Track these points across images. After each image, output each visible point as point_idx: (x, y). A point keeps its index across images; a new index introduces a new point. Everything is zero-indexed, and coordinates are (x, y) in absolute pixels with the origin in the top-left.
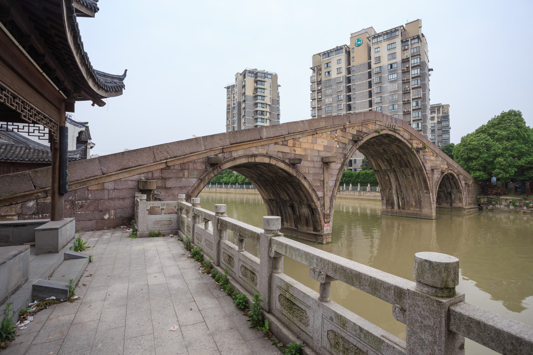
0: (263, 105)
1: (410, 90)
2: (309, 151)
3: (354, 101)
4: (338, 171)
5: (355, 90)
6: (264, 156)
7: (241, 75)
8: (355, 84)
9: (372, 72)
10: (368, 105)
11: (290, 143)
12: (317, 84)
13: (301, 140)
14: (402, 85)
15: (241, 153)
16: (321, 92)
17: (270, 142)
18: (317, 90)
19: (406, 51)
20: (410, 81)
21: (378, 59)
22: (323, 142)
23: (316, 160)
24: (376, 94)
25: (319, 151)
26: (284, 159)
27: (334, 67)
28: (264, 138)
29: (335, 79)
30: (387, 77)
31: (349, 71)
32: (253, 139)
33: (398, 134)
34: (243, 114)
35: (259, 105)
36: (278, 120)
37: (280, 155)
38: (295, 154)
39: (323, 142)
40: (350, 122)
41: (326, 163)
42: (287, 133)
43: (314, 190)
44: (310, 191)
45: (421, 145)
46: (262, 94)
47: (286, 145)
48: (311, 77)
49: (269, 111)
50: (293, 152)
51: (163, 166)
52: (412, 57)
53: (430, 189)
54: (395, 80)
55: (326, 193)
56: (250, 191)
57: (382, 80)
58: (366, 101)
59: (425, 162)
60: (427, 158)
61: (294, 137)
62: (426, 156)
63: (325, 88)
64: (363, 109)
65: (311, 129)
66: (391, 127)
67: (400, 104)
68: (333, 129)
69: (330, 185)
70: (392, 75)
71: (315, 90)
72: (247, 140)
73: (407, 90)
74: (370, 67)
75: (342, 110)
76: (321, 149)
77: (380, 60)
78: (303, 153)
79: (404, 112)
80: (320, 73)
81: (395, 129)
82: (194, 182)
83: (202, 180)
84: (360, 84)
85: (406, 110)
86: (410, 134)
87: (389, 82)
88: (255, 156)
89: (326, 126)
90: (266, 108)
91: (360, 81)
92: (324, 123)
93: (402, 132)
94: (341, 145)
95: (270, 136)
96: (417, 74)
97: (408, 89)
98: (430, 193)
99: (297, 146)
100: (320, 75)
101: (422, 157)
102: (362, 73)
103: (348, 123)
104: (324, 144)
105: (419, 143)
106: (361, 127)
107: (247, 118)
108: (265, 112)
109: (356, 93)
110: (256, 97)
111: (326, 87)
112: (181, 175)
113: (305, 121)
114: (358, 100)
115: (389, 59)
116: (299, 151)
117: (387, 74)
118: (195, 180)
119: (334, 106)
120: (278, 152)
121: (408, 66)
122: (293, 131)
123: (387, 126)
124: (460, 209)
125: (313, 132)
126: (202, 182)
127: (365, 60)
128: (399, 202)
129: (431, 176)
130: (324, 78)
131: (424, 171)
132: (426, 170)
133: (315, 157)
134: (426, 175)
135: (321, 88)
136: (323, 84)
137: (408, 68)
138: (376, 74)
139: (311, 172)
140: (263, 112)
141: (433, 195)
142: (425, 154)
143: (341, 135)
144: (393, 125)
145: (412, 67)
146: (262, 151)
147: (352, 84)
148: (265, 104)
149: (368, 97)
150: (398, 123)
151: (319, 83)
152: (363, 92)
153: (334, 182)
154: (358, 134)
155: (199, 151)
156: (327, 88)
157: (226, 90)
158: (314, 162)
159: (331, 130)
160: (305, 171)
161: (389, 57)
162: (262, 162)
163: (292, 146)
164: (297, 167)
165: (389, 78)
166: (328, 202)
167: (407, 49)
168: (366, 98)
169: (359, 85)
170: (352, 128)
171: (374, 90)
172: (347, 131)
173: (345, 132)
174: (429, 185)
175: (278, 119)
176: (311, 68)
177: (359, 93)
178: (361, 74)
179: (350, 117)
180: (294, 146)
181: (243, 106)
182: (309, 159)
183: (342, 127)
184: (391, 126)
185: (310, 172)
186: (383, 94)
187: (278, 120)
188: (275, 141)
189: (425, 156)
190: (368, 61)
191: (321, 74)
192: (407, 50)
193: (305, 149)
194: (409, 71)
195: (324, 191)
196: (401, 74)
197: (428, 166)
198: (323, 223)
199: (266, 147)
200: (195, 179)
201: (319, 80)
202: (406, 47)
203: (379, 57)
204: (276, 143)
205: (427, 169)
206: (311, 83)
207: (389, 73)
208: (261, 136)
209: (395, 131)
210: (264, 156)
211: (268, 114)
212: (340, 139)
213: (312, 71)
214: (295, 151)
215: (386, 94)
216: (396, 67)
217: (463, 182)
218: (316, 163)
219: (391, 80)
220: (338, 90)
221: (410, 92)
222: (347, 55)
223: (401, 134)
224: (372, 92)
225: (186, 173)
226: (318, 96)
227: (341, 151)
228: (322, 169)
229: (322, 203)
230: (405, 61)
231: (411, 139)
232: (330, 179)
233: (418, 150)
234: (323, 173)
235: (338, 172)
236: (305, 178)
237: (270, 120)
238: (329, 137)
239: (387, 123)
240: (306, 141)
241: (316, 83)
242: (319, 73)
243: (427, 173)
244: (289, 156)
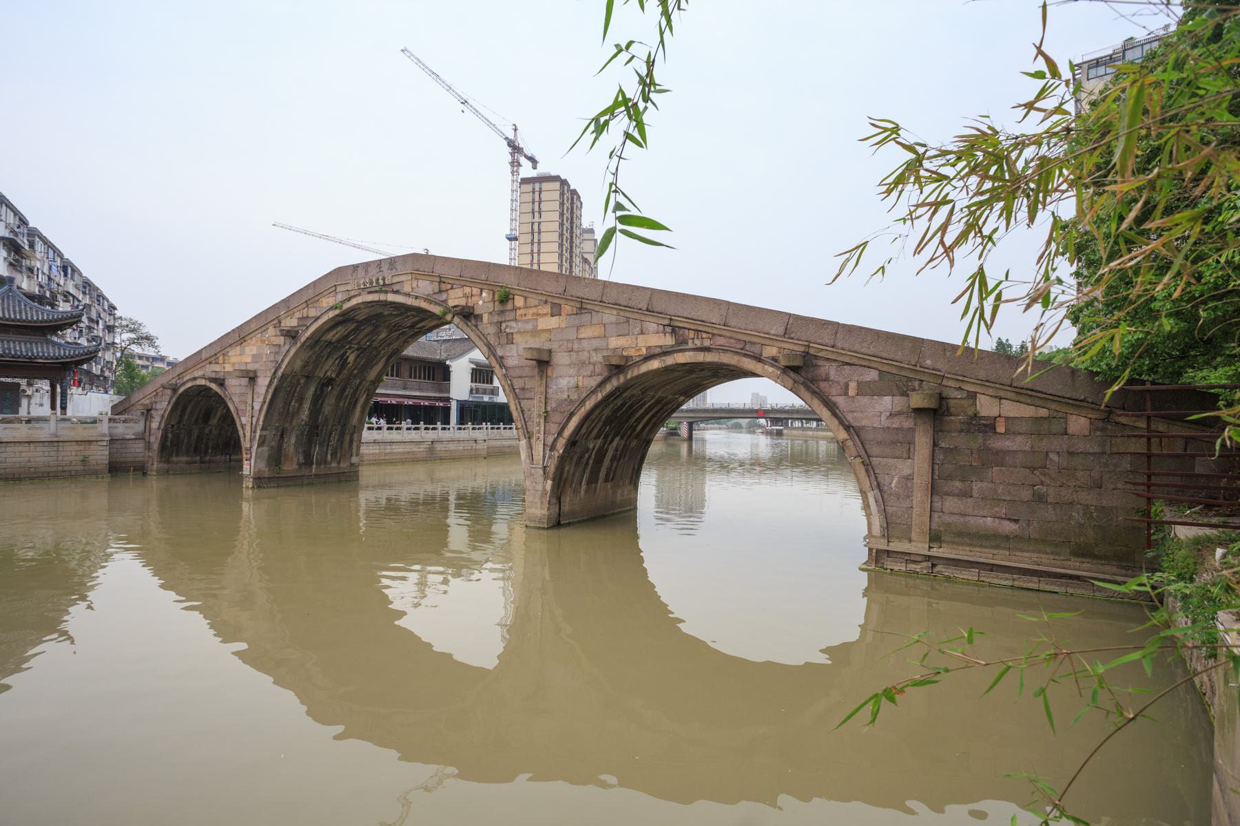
13: (229, 354)
25: (246, 363)
33: (397, 292)
39: (251, 350)
41: (252, 378)
45: (484, 294)
47: (218, 363)
51: (155, 393)
59: (504, 341)
60: (513, 327)
62: (513, 324)
66: (374, 284)
76: (249, 360)
81: (384, 285)
88: (195, 379)
93: (409, 283)
94: (273, 349)
104: (253, 353)
105: (476, 291)
106: (305, 311)
123: (362, 286)
142: (510, 316)
143: (274, 334)
144: (378, 279)
154: (301, 323)
184: (371, 283)
189: (504, 325)
199: (204, 369)
204: (210, 363)
205: (510, 362)
209: (385, 288)
214: (224, 368)
223: (407, 289)
227: (272, 358)
231: (440, 291)
236: (231, 399)
239: (362, 282)
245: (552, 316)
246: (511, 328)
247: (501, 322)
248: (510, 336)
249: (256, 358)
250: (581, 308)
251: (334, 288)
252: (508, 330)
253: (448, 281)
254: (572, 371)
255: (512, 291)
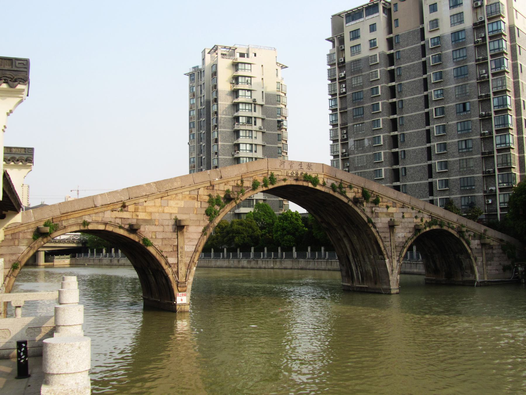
0: (250, 106)
1: (488, 77)
2: (157, 214)
3: (400, 96)
4: (201, 234)
5: (402, 78)
6: (98, 223)
7: (209, 53)
8: (401, 66)
9: (426, 46)
10: (423, 104)
11: (131, 208)
12: (339, 68)
14: (475, 69)
15: (71, 222)
16: (345, 81)
17: (105, 209)
18: (340, 79)
19: (479, 10)
20: (487, 62)
21: (435, 24)
22: (177, 204)
23: (167, 224)
24: (433, 85)
26: (123, 225)
27: (366, 36)
28: (98, 206)
29: (367, 59)
30: (451, 55)
31: (390, 43)
32: (85, 208)
34: (213, 123)
35: (241, 106)
36: (279, 132)
37: (119, 221)
38: (137, 219)
40: (221, 178)
42: (128, 198)
43: (163, 256)
44: (158, 257)
46: (247, 87)
48: (328, 55)
49: (260, 115)
50: (135, 217)
52: (489, 19)
53: (385, 253)
54: (463, 60)
55: (180, 259)
56: (220, 263)
57: (443, 60)
58: (421, 97)
59: (374, 215)
61: (136, 202)
62: (378, 208)
63: (351, 75)
64: (415, 112)
65: (159, 191)
67: (473, 102)
68: (194, 188)
69: (188, 250)
70: (458, 52)
71: (336, 79)
72: (79, 209)
73: (484, 77)
74: (423, 38)
75: (380, 114)
77: (437, 26)
78: (147, 217)
79: (481, 116)
80: (343, 48)
82: (24, 250)
83: (31, 248)
84: (409, 68)
85: (484, 113)
86: (340, 181)
87: (454, 64)
89: (183, 185)
90: (255, 111)
91: (409, 62)
92: (179, 183)
95: (106, 203)
96: (499, 49)
97: (486, 75)
98: (385, 259)
99: (140, 211)
100: (343, 52)
101: (368, 210)
102: (412, 48)
103: (217, 179)
104: (179, 206)
107: (221, 131)
108: (253, 119)
109: (403, 82)
110: (235, 93)
111: (352, 73)
112: (12, 243)
113: (151, 184)
114: (406, 96)
115: (453, 22)
116: (142, 216)
117: (451, 50)
118: (25, 247)
119: (367, 107)
120: (116, 218)
121: (483, 35)
122: (135, 196)
123: (290, 175)
124: (471, 284)
125: (163, 194)
126: (31, 249)
127: (414, 25)
128: (358, 273)
129: (388, 235)
130: (349, 58)
131: (372, 229)
132: (375, 227)
133: (165, 221)
134: (376, 234)
135: (345, 75)
136: (347, 68)
137: (484, 38)
138: (433, 50)
139: (160, 236)
140: (249, 119)
141: (391, 262)
145: (490, 38)
146: (94, 218)
147: (396, 67)
148: (253, 105)
149: (423, 89)
150: (314, 169)
151: (342, 65)
152: (414, 81)
153: (194, 247)
155: (29, 223)
156: (354, 74)
157: (188, 78)
158: (162, 225)
159: (189, 189)
160: (151, 236)
161: (453, 19)
162: (96, 229)
163: (133, 210)
164: (139, 233)
165: (455, 57)
166: (182, 269)
167: (480, 7)
168: (420, 91)
169: (408, 68)
170: (224, 184)
171: (431, 77)
172: (215, 188)
173: (213, 189)
174: (383, 249)
175: (278, 129)
176: (328, 40)
177: (408, 83)
178: (409, 50)
179: (222, 171)
180: (136, 210)
181: (214, 108)
182: (157, 223)
183: (209, 184)
185: (157, 237)
186: (446, 85)
187: (279, 132)
188: (112, 207)
189: (374, 209)
190: (421, 27)
191: (344, 50)
192: (482, 8)
193: (151, 213)
194: (486, 44)
195: (178, 257)
196: (473, 49)
197: (381, 222)
198: (176, 292)
199: (101, 215)
200: (25, 247)
201: (341, 60)
202: (479, 4)
203: (436, 20)
205: (378, 225)
206: (331, 65)
207: (453, 48)
208: (95, 204)
210: (98, 223)
211: (259, 122)
212: (204, 198)
213: (331, 43)
214: (137, 216)
215: (451, 84)
216: (463, 37)
217: (475, 243)
218: (166, 227)
219: (458, 60)
220: (372, 78)
221: (489, 81)
222: (386, 16)
224: (428, 81)
225: (16, 242)
226: (340, 88)
228: (176, 233)
229: (175, 270)
230: (479, 26)
232: (188, 244)
233: (356, 201)
234: (178, 238)
235: (199, 237)
237: (263, 133)
238: (187, 198)
239: (290, 172)
240: (153, 204)
241: (336, 66)
242: (341, 47)
243: (378, 232)
244: (130, 222)
245: (393, 207)
246: (377, 210)
247: (372, 207)
248: (377, 214)
249: (181, 210)
250: (403, 205)
251: (267, 172)
252: (376, 211)
253: (345, 183)
254: (402, 230)
255: (380, 195)
